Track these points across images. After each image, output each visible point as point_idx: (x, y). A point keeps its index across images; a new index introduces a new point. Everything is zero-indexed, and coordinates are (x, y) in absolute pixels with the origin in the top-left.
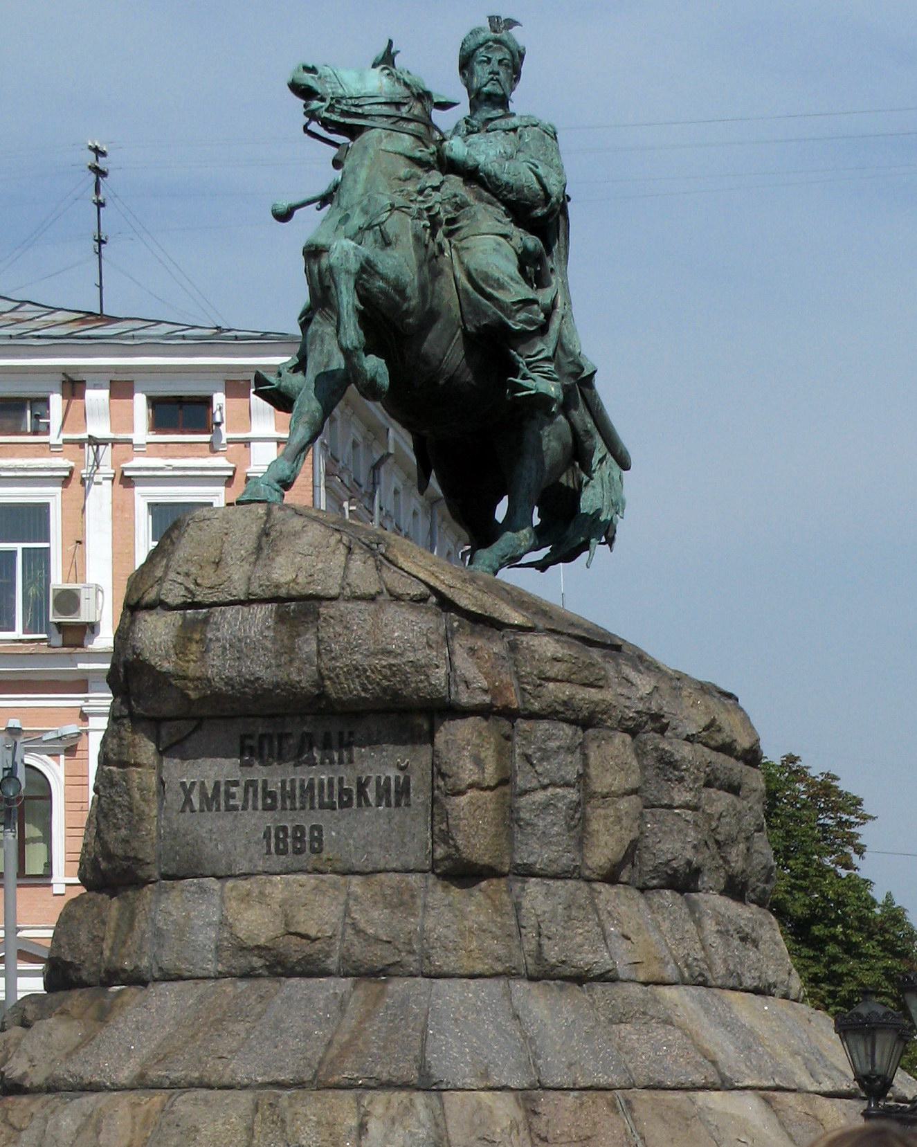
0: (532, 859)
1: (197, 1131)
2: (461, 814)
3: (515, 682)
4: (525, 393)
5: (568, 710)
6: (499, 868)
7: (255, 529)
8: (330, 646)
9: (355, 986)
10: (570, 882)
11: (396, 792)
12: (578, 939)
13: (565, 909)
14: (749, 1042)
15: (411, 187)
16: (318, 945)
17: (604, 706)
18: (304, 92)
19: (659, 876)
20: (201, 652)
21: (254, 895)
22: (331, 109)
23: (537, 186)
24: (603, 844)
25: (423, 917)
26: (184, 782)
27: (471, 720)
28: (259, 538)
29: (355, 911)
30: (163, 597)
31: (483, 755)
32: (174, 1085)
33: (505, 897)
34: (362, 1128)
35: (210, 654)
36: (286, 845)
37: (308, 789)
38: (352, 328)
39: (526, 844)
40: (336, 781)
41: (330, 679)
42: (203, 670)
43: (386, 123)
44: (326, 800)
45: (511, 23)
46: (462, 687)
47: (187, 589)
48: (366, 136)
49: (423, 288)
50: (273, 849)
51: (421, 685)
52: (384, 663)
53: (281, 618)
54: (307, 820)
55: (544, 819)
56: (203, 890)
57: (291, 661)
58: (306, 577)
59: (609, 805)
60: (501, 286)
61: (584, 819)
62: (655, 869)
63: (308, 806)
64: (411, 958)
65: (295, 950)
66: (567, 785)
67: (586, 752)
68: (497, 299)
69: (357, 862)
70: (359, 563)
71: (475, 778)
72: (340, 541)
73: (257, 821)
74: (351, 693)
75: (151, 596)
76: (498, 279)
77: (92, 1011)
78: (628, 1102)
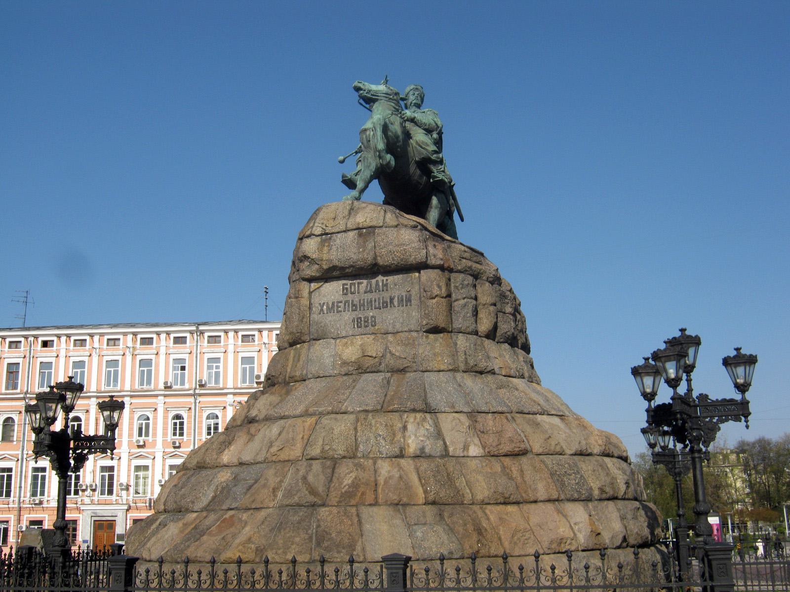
1: (333, 429)
9: (392, 375)
11: (406, 301)
16: (377, 360)
23: (434, 124)
27: (436, 271)
31: (441, 284)
34: (405, 428)
36: (361, 324)
47: (322, 228)
50: (356, 326)
53: (360, 235)
56: (328, 344)
57: (364, 251)
60: (428, 145)
65: (369, 362)
69: (390, 329)
71: (438, 292)
73: (348, 316)
75: (308, 233)
77: (284, 391)
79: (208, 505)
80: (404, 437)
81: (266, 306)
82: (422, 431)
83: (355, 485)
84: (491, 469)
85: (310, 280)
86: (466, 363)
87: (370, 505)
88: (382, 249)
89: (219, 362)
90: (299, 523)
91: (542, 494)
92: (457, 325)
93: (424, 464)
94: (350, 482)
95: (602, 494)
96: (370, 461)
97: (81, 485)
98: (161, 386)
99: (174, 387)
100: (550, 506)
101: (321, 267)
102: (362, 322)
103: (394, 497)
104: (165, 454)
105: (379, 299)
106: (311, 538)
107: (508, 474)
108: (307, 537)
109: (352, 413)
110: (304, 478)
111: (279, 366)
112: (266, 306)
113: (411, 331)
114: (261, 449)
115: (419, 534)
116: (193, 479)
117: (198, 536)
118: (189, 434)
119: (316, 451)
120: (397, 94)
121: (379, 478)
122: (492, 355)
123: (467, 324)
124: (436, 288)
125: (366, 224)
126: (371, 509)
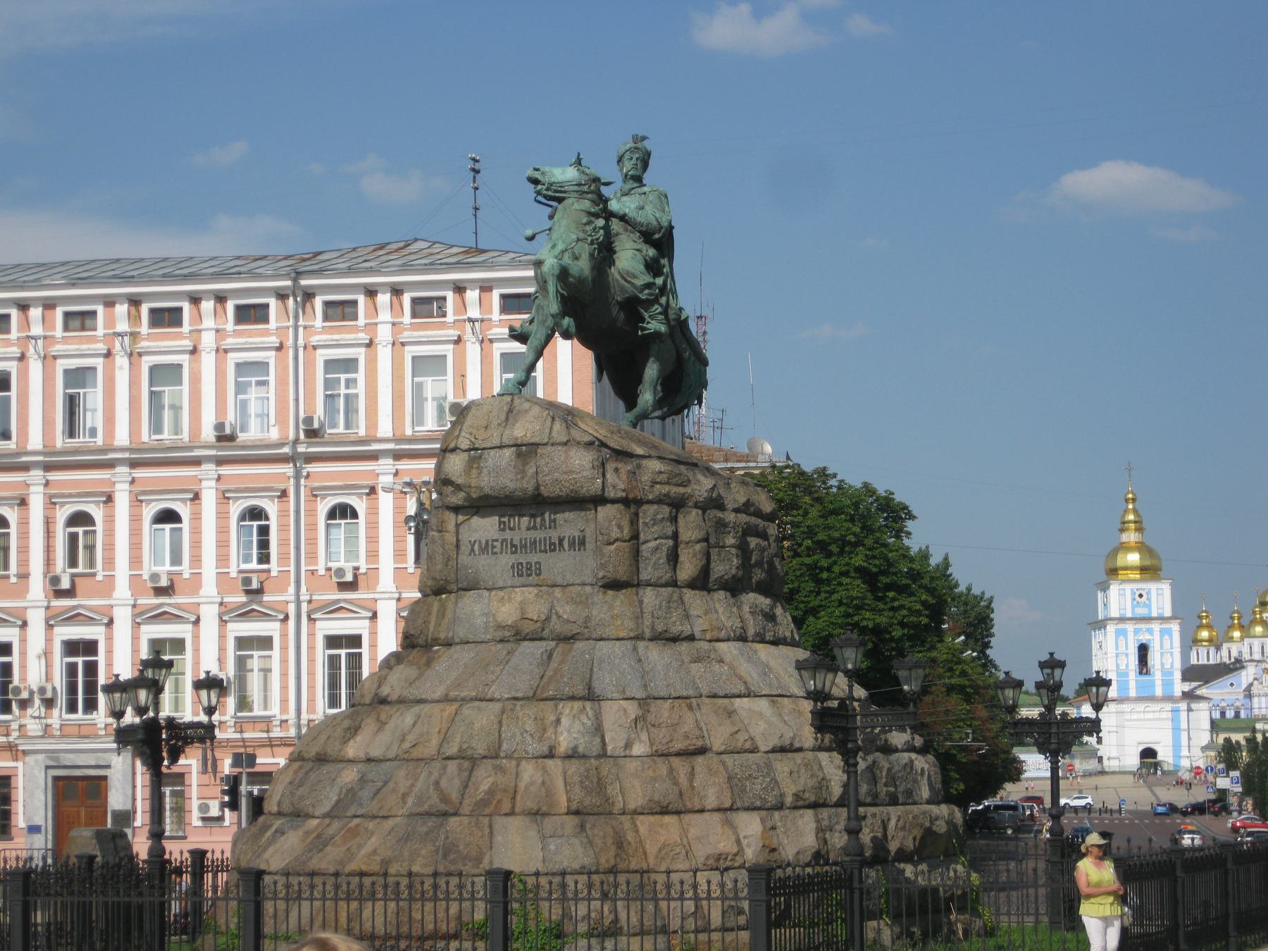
9: (557, 646)
14: (766, 670)
15: (588, 228)
16: (539, 624)
22: (548, 189)
23: (655, 223)
28: (508, 414)
32: (463, 699)
34: (558, 721)
43: (575, 195)
45: (644, 138)
48: (565, 202)
53: (519, 455)
54: (534, 558)
56: (481, 596)
57: (523, 478)
60: (635, 277)
64: (586, 630)
65: (528, 628)
66: (667, 538)
69: (559, 581)
73: (507, 560)
75: (452, 445)
77: (424, 660)
78: (698, 705)
79: (331, 811)
80: (556, 733)
81: (476, 209)
82: (577, 726)
83: (491, 792)
84: (654, 771)
85: (456, 509)
86: (653, 628)
87: (506, 815)
88: (546, 476)
89: (356, 371)
90: (427, 834)
91: (711, 802)
92: (644, 576)
93: (574, 767)
94: (486, 788)
95: (797, 801)
96: (514, 763)
97: (17, 691)
98: (208, 434)
99: (242, 437)
100: (717, 816)
103: (531, 805)
104: (223, 609)
105: (545, 539)
106: (437, 851)
107: (675, 778)
108: (434, 849)
109: (499, 700)
110: (437, 783)
111: (420, 621)
112: (476, 209)
113: (584, 584)
114: (392, 743)
115: (552, 847)
116: (313, 776)
117: (321, 847)
118: (283, 558)
119: (452, 749)
121: (519, 784)
122: (693, 612)
123: (658, 574)
124: (615, 529)
125: (526, 440)
126: (505, 819)
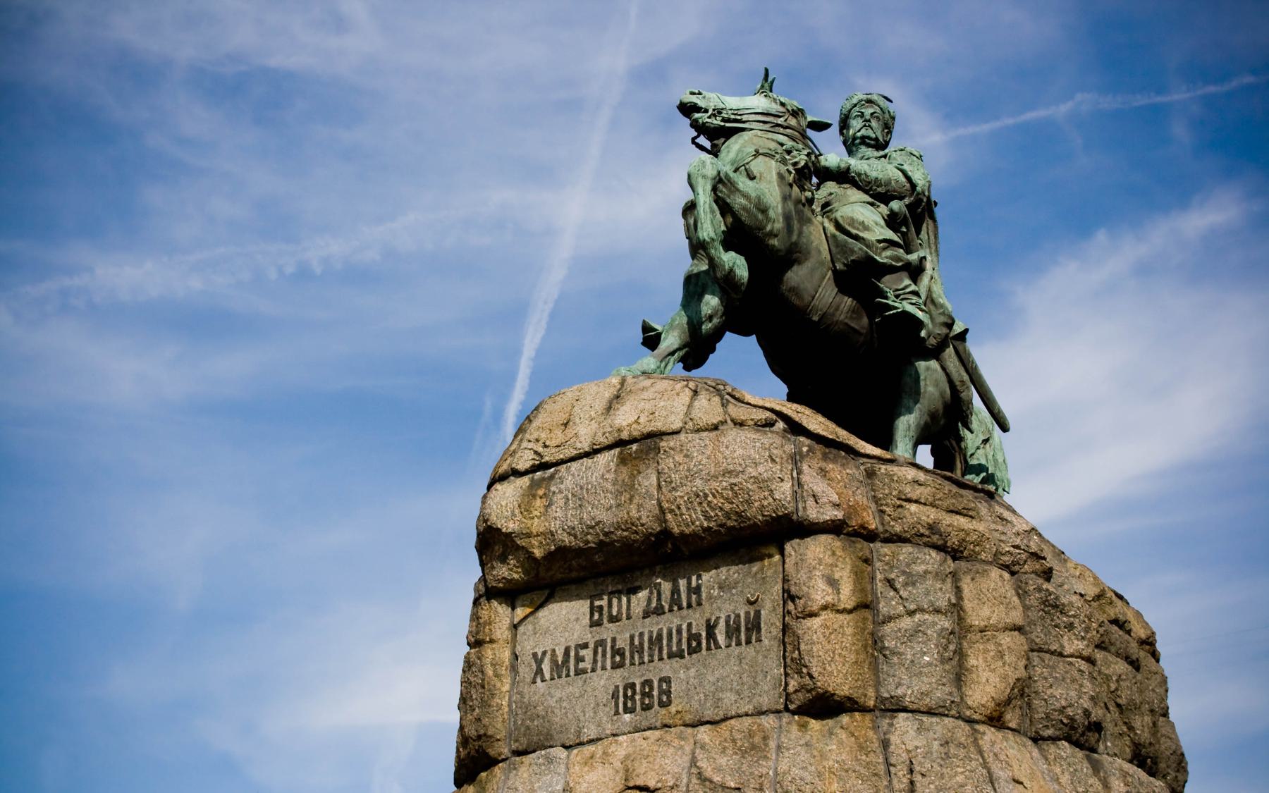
0: (900, 692)
2: (814, 638)
3: (873, 506)
4: (895, 311)
5: (934, 534)
6: (861, 701)
7: (608, 394)
8: (670, 477)
10: (946, 720)
11: (747, 629)
12: (958, 778)
13: (941, 745)
17: (975, 537)
18: (687, 109)
19: (1053, 726)
20: (545, 506)
21: (598, 756)
23: (903, 179)
24: (984, 680)
25: (777, 760)
26: (536, 653)
29: (702, 759)
30: (514, 466)
31: (837, 576)
33: (871, 733)
35: (554, 507)
37: (656, 641)
38: (709, 222)
39: (894, 676)
40: (684, 627)
41: (671, 511)
42: (547, 524)
44: (674, 649)
46: (811, 502)
47: (536, 452)
49: (787, 218)
51: (766, 503)
52: (724, 484)
53: (623, 461)
55: (912, 648)
56: (550, 761)
57: (631, 500)
58: (648, 416)
59: (988, 640)
60: (866, 228)
61: (961, 654)
62: (1048, 716)
63: (656, 658)
66: (937, 611)
67: (959, 585)
68: (863, 239)
69: (709, 714)
70: (703, 401)
71: (829, 599)
72: (687, 386)
73: (604, 681)
74: (693, 524)
75: (504, 467)
76: (863, 221)
101: (530, 556)
102: (638, 697)
113: (761, 713)
120: (796, 113)
124: (821, 585)
